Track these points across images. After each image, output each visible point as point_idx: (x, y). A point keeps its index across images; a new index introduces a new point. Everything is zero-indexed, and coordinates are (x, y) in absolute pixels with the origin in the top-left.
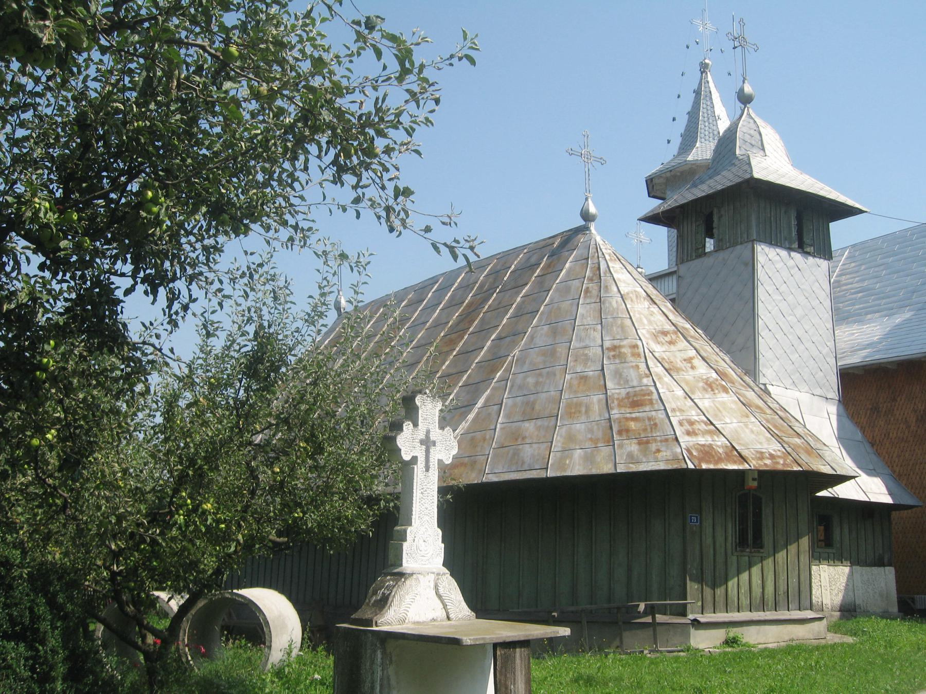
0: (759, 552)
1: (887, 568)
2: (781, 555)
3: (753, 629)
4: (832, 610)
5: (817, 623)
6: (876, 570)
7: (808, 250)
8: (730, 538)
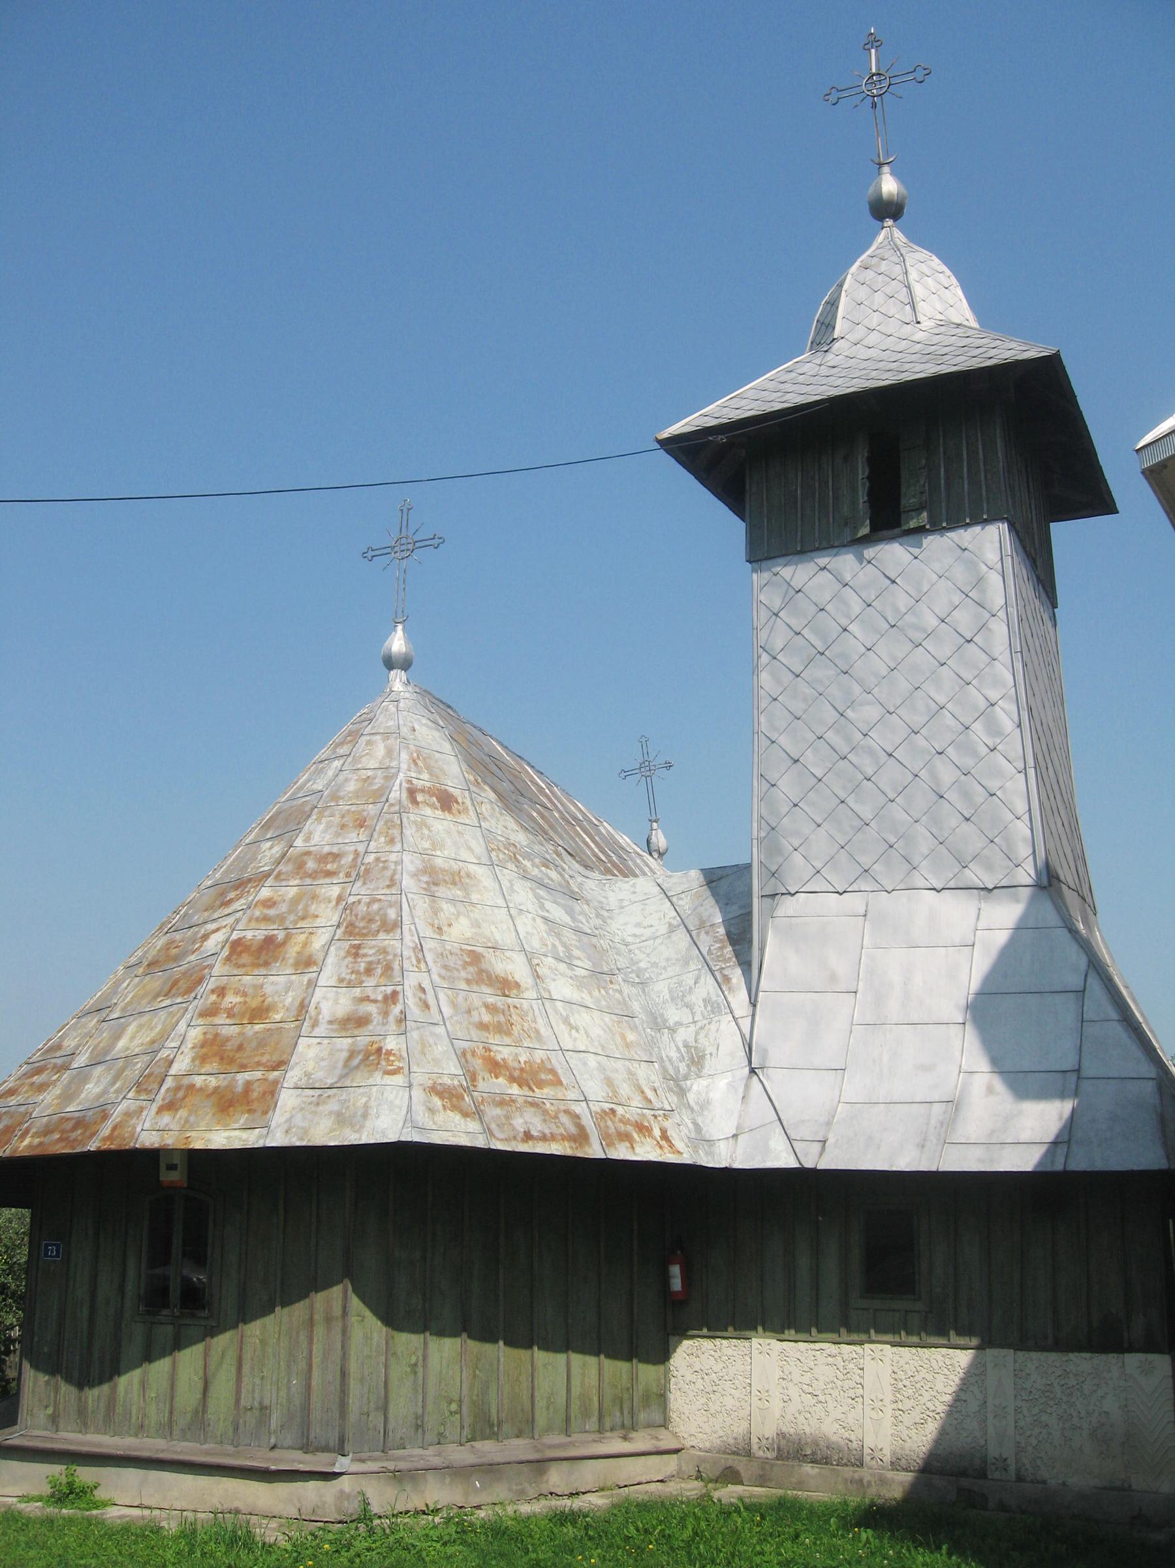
0: (193, 1316)
1: (1133, 1360)
2: (254, 1329)
3: (132, 1475)
4: (895, 1465)
5: (312, 1485)
6: (1082, 1362)
7: (913, 524)
8: (130, 1287)
